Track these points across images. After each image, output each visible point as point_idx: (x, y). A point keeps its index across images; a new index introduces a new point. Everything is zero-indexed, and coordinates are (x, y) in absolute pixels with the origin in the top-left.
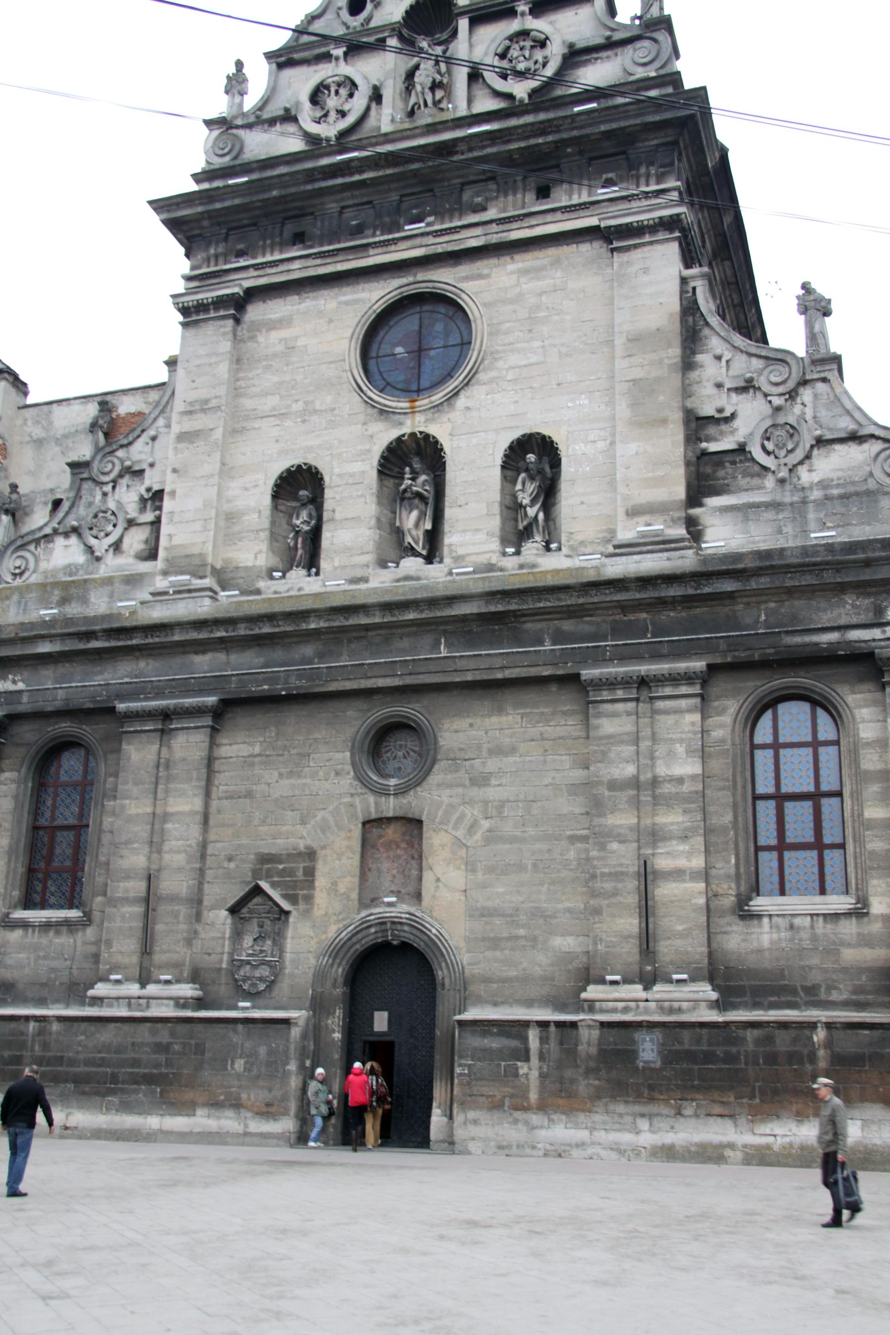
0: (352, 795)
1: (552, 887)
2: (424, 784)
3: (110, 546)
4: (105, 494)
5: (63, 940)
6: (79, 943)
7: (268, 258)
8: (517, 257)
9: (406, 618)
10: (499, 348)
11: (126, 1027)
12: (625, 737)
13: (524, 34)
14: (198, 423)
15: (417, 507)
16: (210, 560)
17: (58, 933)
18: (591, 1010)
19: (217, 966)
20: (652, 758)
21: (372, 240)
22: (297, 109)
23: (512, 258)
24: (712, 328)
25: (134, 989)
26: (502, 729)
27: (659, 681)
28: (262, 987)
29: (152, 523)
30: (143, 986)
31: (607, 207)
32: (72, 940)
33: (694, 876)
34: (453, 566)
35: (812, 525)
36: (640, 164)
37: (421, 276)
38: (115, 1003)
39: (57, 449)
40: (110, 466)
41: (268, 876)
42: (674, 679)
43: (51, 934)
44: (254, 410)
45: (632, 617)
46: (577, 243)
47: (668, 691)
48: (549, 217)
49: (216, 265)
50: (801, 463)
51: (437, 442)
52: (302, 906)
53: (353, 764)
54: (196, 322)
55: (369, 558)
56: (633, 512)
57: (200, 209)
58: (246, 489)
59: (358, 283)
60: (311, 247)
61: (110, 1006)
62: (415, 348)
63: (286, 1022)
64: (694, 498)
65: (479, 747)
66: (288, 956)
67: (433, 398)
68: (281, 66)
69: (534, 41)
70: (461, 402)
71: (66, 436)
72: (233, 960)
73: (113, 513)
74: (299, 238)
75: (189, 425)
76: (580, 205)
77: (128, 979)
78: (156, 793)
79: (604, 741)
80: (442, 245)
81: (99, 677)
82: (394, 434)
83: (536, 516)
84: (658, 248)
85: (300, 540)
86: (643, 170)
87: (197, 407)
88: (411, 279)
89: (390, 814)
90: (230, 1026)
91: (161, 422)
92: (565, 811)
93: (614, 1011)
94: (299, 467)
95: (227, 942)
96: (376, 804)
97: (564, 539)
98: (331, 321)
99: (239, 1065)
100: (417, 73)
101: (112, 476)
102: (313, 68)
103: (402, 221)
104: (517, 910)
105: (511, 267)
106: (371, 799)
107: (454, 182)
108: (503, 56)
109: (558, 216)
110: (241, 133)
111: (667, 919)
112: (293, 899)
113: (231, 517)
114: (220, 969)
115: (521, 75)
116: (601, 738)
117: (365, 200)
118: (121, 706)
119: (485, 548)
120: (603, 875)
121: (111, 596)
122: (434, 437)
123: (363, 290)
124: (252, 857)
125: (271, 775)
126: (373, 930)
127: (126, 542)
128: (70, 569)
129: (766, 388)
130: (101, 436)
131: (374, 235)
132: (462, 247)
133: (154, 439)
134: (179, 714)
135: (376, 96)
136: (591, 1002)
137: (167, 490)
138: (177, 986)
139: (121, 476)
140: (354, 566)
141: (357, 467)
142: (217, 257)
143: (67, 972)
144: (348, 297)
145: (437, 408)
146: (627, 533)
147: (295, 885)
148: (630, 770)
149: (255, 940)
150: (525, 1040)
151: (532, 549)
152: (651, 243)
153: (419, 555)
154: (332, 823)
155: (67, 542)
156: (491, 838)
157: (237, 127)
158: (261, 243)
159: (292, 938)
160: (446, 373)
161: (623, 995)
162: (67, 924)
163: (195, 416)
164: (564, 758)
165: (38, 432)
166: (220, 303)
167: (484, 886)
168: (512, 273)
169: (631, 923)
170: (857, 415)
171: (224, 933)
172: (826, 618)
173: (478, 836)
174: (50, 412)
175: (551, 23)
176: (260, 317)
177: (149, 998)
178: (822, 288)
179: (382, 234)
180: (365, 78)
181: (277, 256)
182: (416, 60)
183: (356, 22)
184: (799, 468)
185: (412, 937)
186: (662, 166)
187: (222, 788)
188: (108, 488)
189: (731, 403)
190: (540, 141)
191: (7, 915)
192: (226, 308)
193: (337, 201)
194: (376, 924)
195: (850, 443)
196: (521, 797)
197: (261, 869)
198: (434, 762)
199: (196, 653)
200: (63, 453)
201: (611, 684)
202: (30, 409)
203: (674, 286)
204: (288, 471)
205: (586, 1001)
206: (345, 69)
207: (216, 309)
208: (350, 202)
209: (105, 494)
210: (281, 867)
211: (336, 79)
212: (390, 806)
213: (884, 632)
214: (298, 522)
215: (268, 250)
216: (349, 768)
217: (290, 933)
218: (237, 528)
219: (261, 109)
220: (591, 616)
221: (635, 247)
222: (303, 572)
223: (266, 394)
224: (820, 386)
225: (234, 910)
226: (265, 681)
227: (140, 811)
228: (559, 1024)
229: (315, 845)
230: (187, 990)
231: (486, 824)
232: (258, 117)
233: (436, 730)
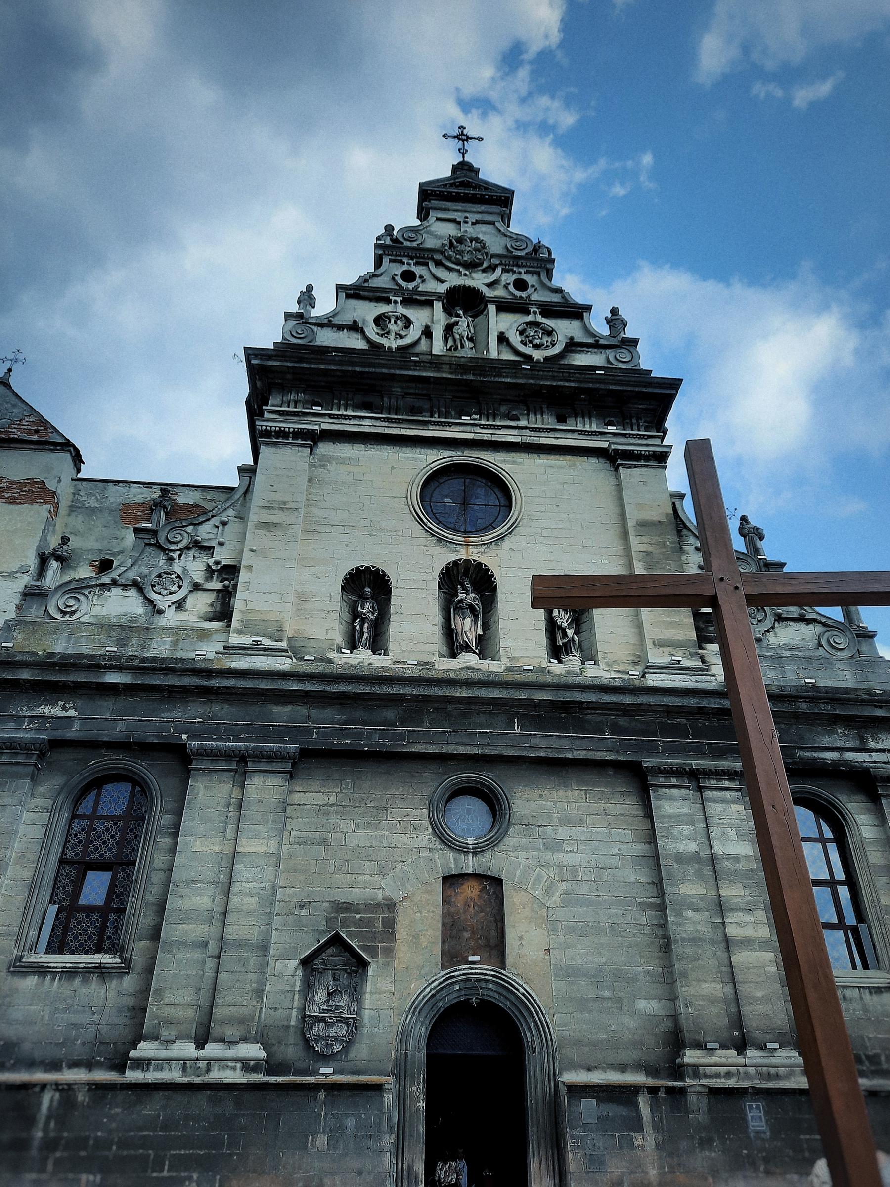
0: (431, 850)
1: (630, 950)
2: (501, 847)
3: (173, 603)
6: (112, 994)
7: (340, 413)
8: (542, 456)
9: (490, 695)
11: (179, 1097)
12: (685, 818)
13: (535, 324)
14: (275, 517)
15: (469, 617)
17: (85, 981)
18: (696, 1075)
19: (286, 1023)
20: (709, 839)
21: (433, 419)
22: (364, 323)
23: (538, 456)
24: (690, 530)
25: (187, 1049)
26: (569, 802)
27: (707, 774)
28: (337, 1048)
29: (218, 591)
30: (200, 1045)
31: (610, 437)
32: (103, 991)
34: (509, 664)
37: (466, 453)
38: (166, 1066)
40: (180, 538)
41: (345, 924)
42: (720, 774)
43: (77, 981)
44: (325, 518)
46: (587, 457)
47: (713, 783)
48: (569, 435)
50: (768, 631)
51: (488, 570)
52: (381, 959)
53: (431, 821)
54: (276, 444)
56: (659, 644)
57: (289, 364)
61: (160, 1068)
62: (460, 500)
63: (378, 1088)
65: (549, 815)
66: (367, 1014)
67: (484, 538)
68: (348, 296)
69: (542, 329)
70: (507, 544)
72: (304, 1017)
73: (179, 577)
74: (367, 406)
75: (266, 517)
76: (592, 432)
77: (180, 1037)
78: (225, 832)
79: (667, 820)
80: (486, 435)
81: (166, 715)
82: (453, 557)
83: (573, 638)
84: (651, 470)
88: (459, 453)
89: (470, 871)
90: (311, 1094)
91: (231, 512)
92: (633, 880)
93: (717, 1075)
94: (367, 568)
95: (297, 996)
96: (455, 859)
97: (600, 657)
98: (393, 468)
99: (322, 1140)
100: (456, 327)
101: (180, 546)
102: (373, 304)
104: (601, 971)
106: (451, 855)
107: (495, 396)
108: (521, 333)
109: (575, 436)
110: (315, 328)
111: (746, 986)
113: (302, 598)
114: (288, 1027)
115: (537, 347)
116: (664, 816)
117: (424, 392)
120: (683, 939)
121: (175, 643)
122: (485, 566)
124: (326, 904)
125: (347, 826)
126: (457, 987)
127: (189, 601)
130: (162, 513)
131: (432, 416)
132: (504, 440)
133: (224, 524)
134: (257, 757)
135: (427, 333)
136: (695, 1067)
137: (243, 563)
138: (242, 1046)
139: (188, 548)
142: (296, 403)
143: (93, 1029)
144: (410, 455)
145: (488, 544)
146: (657, 657)
147: (374, 936)
148: (692, 847)
149: (329, 994)
150: (636, 1105)
151: (573, 662)
152: (646, 466)
153: (475, 653)
154: (412, 876)
156: (568, 900)
157: (310, 324)
158: (336, 401)
159: (372, 993)
160: (488, 524)
161: (723, 1060)
162: (101, 970)
163: (272, 512)
164: (627, 831)
165: (92, 503)
166: (299, 434)
167: (567, 946)
171: (295, 985)
172: (826, 741)
173: (556, 898)
176: (331, 453)
177: (210, 1061)
178: (753, 522)
179: (439, 418)
181: (350, 413)
182: (454, 319)
184: (768, 634)
185: (496, 995)
186: (645, 422)
187: (293, 833)
188: (176, 555)
190: (567, 384)
191: (22, 957)
193: (403, 388)
194: (462, 980)
195: (800, 623)
196: (593, 863)
197: (336, 918)
198: (509, 824)
201: (669, 772)
202: (84, 483)
204: (357, 569)
205: (688, 1065)
206: (401, 310)
208: (412, 391)
209: (171, 559)
210: (358, 917)
212: (469, 864)
213: (870, 756)
215: (342, 408)
216: (426, 824)
217: (369, 987)
218: (308, 606)
219: (333, 316)
220: (642, 716)
221: (635, 466)
225: (306, 963)
226: (347, 736)
227: (207, 849)
228: (670, 1090)
229: (396, 896)
230: (254, 1051)
231: (563, 886)
232: (330, 321)
233: (509, 797)
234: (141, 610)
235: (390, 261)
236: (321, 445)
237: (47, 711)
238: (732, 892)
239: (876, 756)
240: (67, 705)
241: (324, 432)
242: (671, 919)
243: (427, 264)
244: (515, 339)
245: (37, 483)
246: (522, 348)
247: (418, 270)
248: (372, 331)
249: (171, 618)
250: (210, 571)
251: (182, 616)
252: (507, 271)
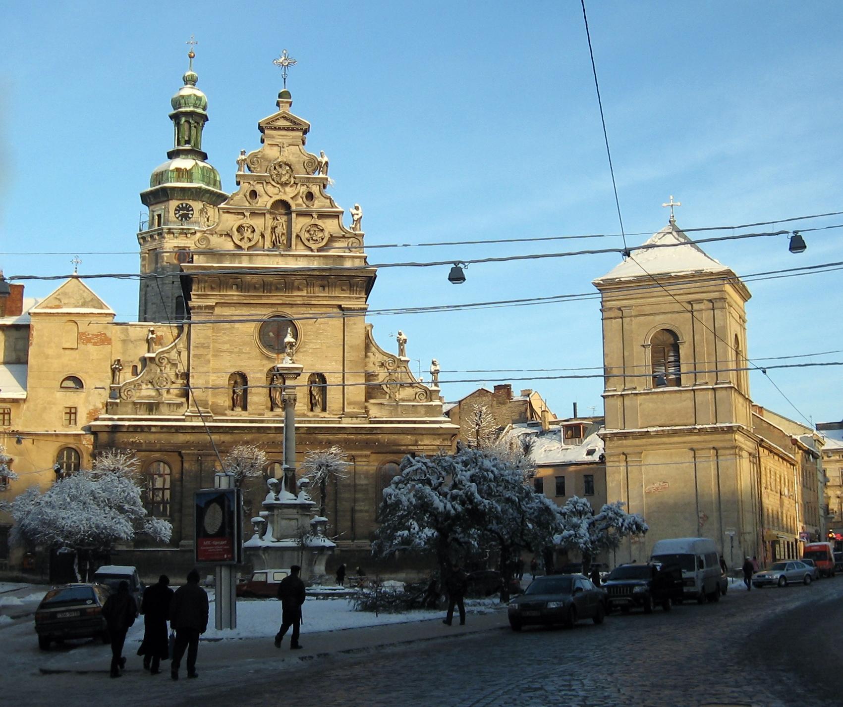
4: (161, 370)
8: (312, 309)
16: (210, 403)
33: (366, 511)
35: (399, 412)
36: (354, 286)
39: (131, 345)
42: (361, 456)
45: (349, 437)
47: (359, 459)
49: (204, 291)
55: (263, 407)
56: (349, 404)
58: (219, 378)
59: (257, 307)
64: (366, 401)
71: (135, 341)
80: (288, 300)
82: (272, 365)
85: (238, 398)
86: (355, 288)
87: (200, 345)
97: (327, 409)
100: (276, 229)
103: (273, 288)
109: (327, 299)
115: (314, 240)
118: (183, 452)
119: (303, 408)
123: (259, 310)
128: (149, 397)
129: (388, 367)
140: (260, 409)
141: (259, 375)
142: (204, 288)
153: (279, 407)
166: (207, 307)
169: (348, 524)
170: (413, 379)
174: (127, 329)
175: (324, 223)
180: (258, 227)
183: (253, 202)
189: (377, 370)
192: (209, 310)
200: (135, 347)
203: (363, 331)
207: (205, 309)
211: (247, 225)
214: (237, 391)
222: (240, 409)
223: (225, 343)
224: (403, 368)
234: (153, 393)
235: (244, 182)
236: (216, 309)
238: (359, 496)
239: (420, 447)
241: (217, 303)
242: (338, 504)
243: (263, 183)
244: (305, 236)
245: (101, 334)
246: (307, 243)
247: (259, 188)
248: (236, 236)
249: (166, 397)
250: (177, 375)
251: (169, 396)
252: (303, 185)
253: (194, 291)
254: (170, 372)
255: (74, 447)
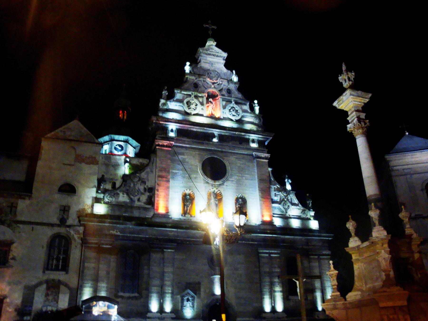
4: (134, 185)
5: (134, 302)
10: (233, 174)
13: (234, 107)
30: (161, 314)
60: (190, 138)
70: (225, 184)
105: (234, 157)
112: (195, 294)
121: (140, 212)
127: (141, 199)
155: (123, 195)
162: (135, 297)
168: (234, 158)
199: (169, 232)
231: (238, 279)
234: (128, 201)
237: (112, 232)
240: (117, 231)
245: (92, 157)
253: (160, 134)
254: (142, 188)
255: (65, 235)
